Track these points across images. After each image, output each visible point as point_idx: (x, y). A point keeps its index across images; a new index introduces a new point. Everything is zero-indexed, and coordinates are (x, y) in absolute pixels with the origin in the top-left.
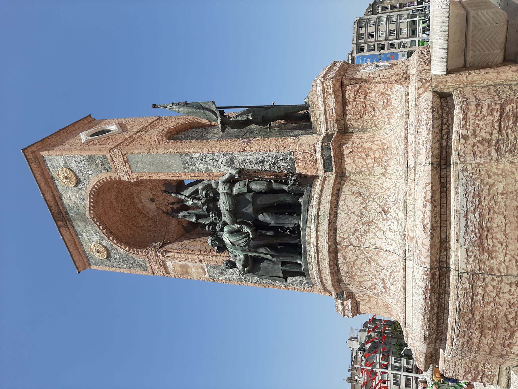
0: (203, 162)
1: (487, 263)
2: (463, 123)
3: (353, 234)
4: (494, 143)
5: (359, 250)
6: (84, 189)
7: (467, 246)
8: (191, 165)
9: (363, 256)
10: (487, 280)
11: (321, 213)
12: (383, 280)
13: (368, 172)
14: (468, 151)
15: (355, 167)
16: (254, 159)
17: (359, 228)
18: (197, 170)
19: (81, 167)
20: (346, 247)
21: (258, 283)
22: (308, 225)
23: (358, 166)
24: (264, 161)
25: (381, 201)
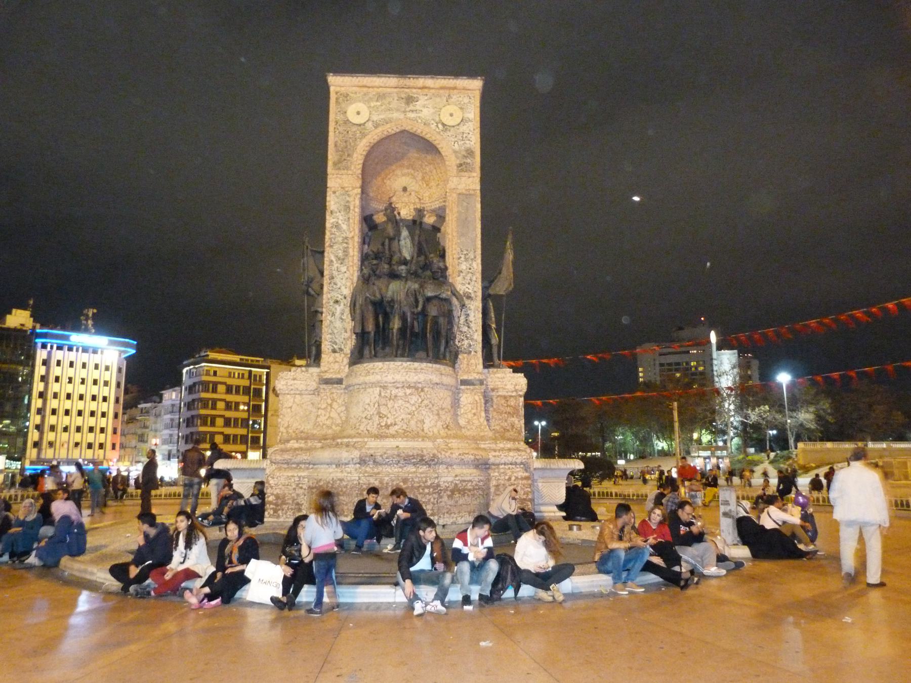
0: (468, 270)
1: (445, 494)
2: (519, 477)
3: (430, 402)
5: (419, 406)
6: (437, 130)
7: (454, 482)
8: (465, 258)
9: (414, 409)
10: (434, 495)
11: (443, 376)
12: (395, 424)
14: (500, 481)
19: (462, 137)
20: (420, 396)
24: (469, 327)
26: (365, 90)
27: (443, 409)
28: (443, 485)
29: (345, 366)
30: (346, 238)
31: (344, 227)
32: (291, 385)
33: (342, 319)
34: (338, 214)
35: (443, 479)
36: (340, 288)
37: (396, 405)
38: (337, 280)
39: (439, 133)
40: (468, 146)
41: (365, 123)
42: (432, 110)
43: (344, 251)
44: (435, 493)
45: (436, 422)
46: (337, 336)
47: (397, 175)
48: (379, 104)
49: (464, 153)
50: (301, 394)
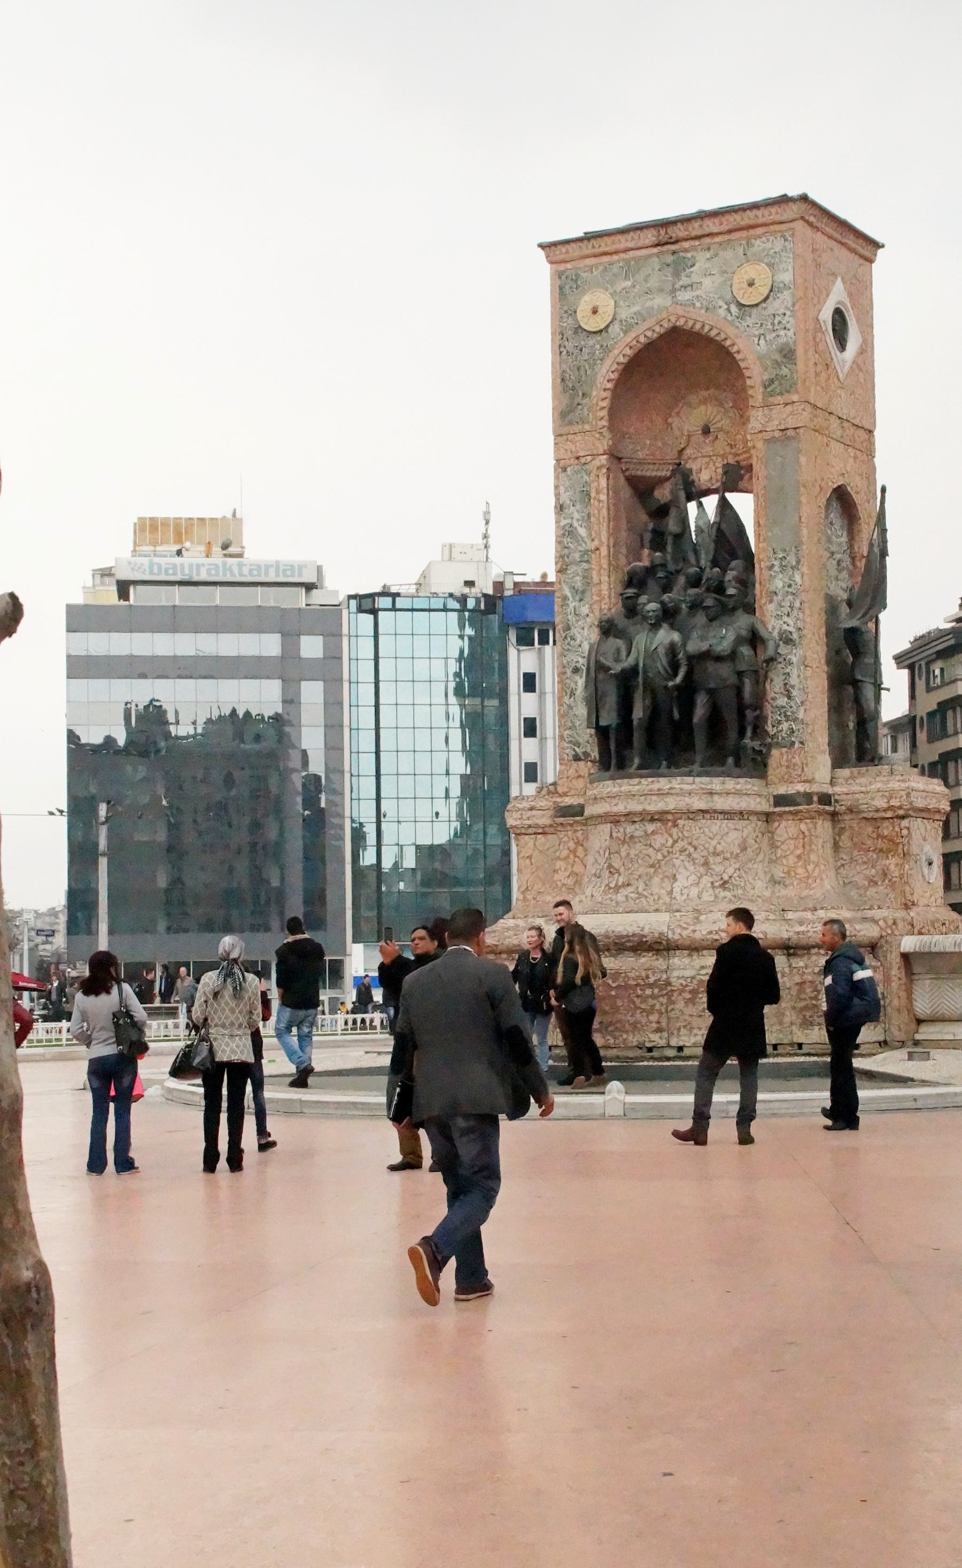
1: (680, 998)
3: (690, 844)
4: (814, 1002)
5: (668, 852)
6: (729, 318)
8: (781, 566)
9: (660, 857)
11: (716, 798)
12: (628, 885)
13: (774, 858)
14: (805, 977)
15: (782, 839)
16: (794, 680)
17: (699, 851)
18: (773, 574)
19: (773, 324)
20: (671, 836)
21: (565, 662)
22: (698, 779)
23: (783, 843)
24: (789, 697)
25: (737, 878)
26: (606, 259)
27: (716, 854)
28: (676, 983)
30: (586, 552)
31: (582, 532)
32: (528, 818)
34: (572, 508)
35: (676, 974)
36: (580, 646)
37: (633, 852)
39: (731, 323)
41: (608, 326)
42: (718, 279)
44: (663, 996)
45: (700, 878)
46: (580, 732)
47: (690, 405)
48: (629, 283)
49: (778, 357)
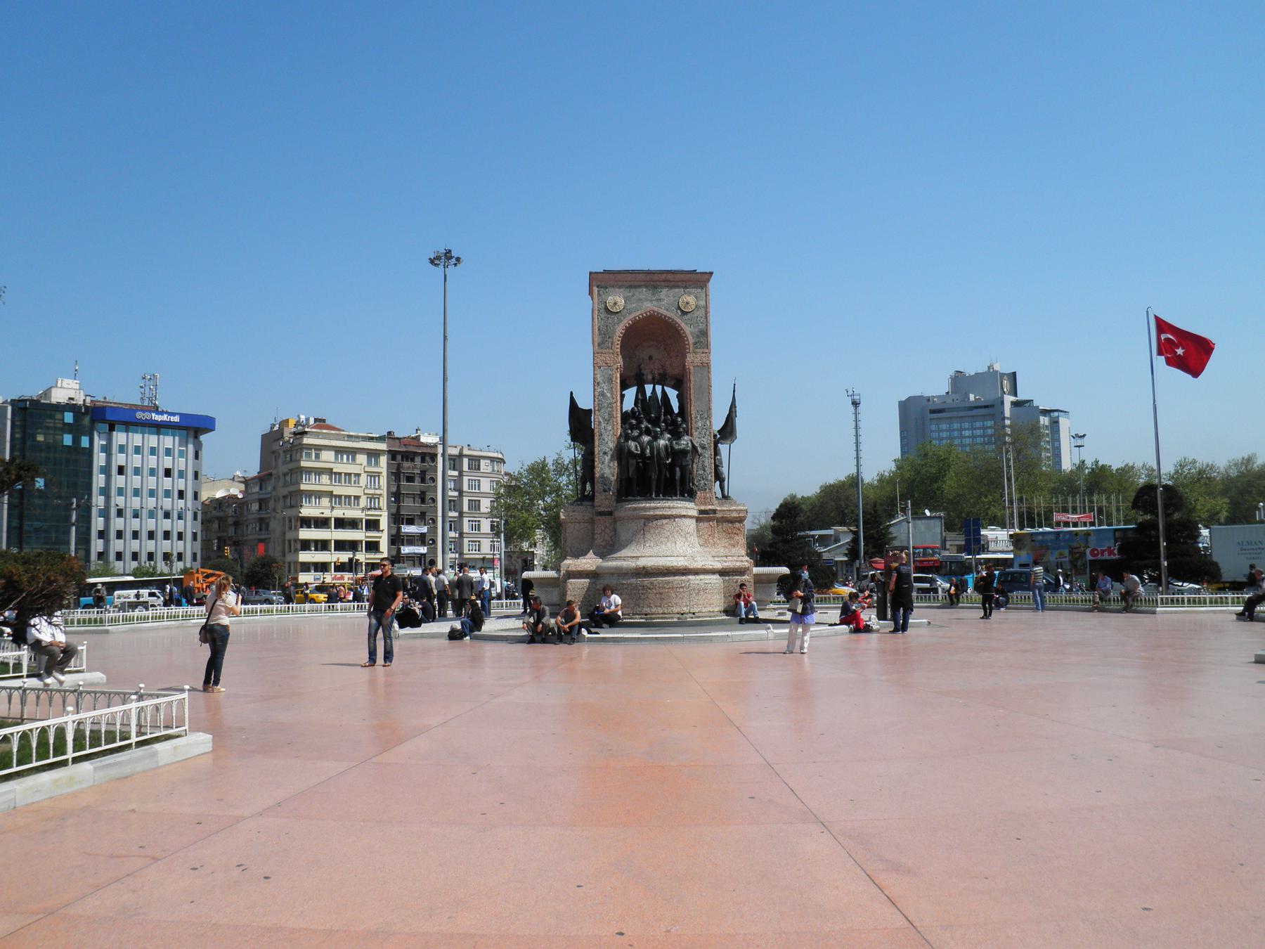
24: (704, 471)
27: (688, 533)
29: (613, 502)
30: (610, 404)
31: (609, 395)
33: (609, 466)
38: (605, 436)
40: (701, 327)
43: (609, 414)
50: (579, 523)
